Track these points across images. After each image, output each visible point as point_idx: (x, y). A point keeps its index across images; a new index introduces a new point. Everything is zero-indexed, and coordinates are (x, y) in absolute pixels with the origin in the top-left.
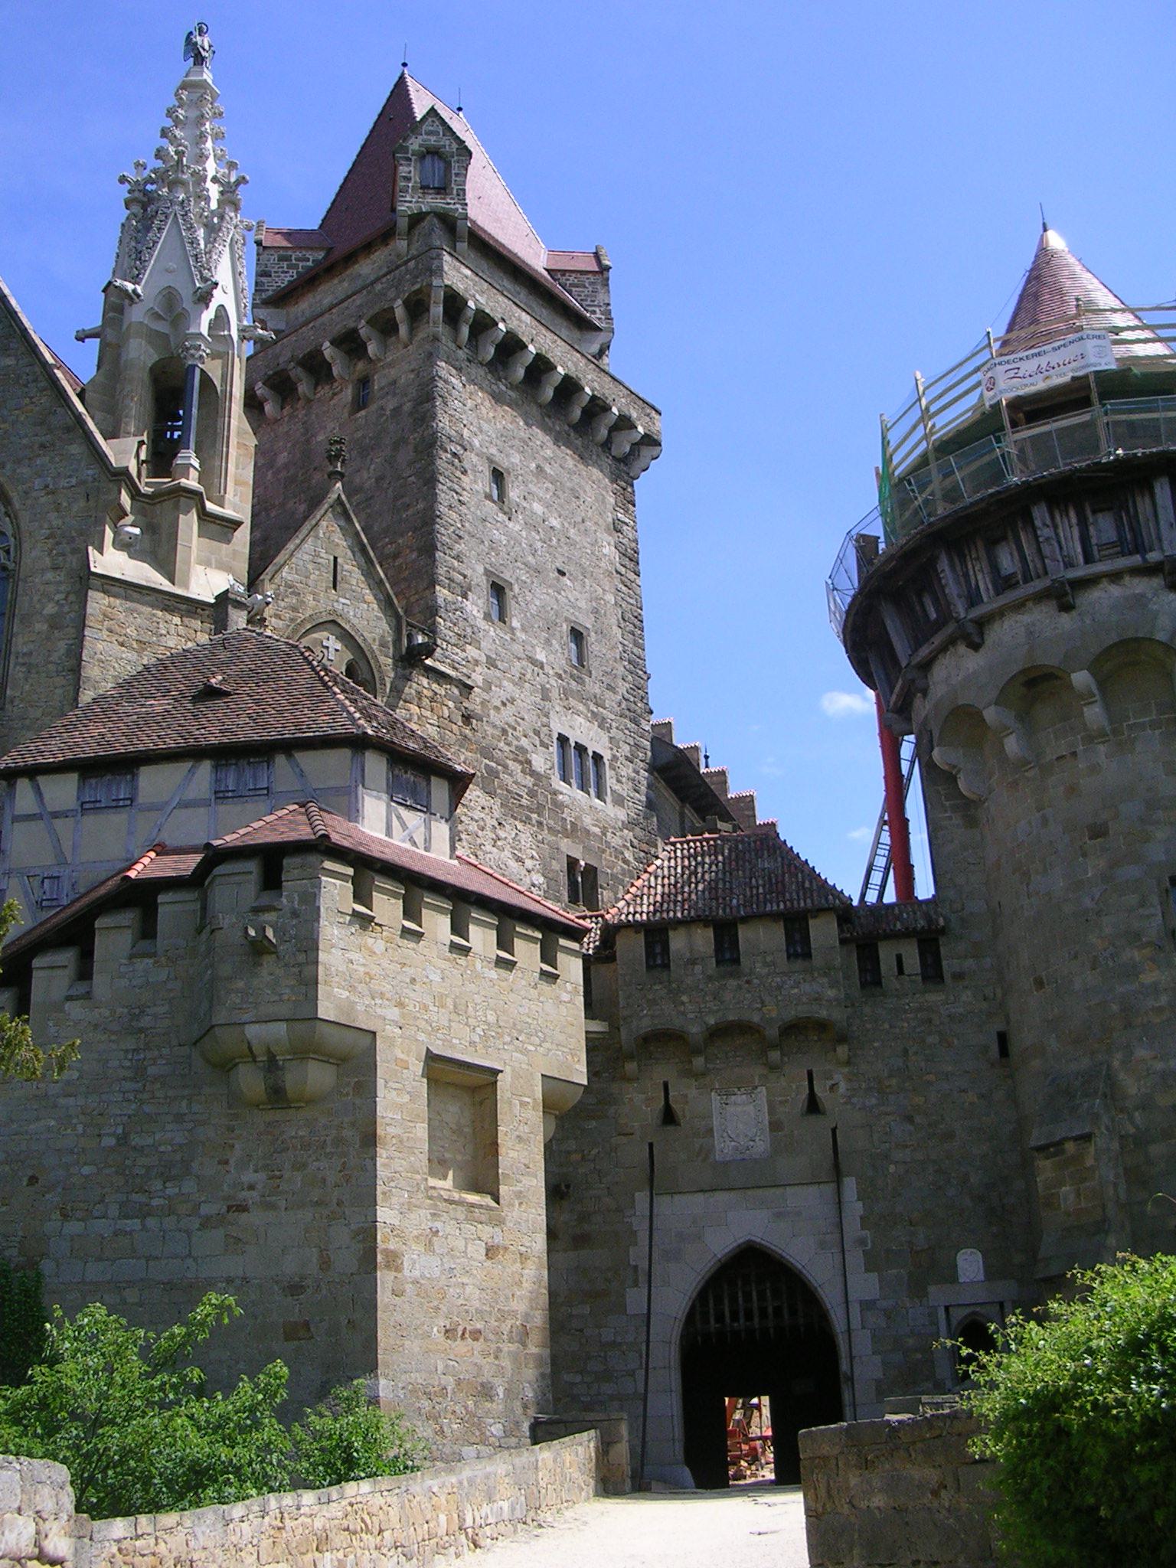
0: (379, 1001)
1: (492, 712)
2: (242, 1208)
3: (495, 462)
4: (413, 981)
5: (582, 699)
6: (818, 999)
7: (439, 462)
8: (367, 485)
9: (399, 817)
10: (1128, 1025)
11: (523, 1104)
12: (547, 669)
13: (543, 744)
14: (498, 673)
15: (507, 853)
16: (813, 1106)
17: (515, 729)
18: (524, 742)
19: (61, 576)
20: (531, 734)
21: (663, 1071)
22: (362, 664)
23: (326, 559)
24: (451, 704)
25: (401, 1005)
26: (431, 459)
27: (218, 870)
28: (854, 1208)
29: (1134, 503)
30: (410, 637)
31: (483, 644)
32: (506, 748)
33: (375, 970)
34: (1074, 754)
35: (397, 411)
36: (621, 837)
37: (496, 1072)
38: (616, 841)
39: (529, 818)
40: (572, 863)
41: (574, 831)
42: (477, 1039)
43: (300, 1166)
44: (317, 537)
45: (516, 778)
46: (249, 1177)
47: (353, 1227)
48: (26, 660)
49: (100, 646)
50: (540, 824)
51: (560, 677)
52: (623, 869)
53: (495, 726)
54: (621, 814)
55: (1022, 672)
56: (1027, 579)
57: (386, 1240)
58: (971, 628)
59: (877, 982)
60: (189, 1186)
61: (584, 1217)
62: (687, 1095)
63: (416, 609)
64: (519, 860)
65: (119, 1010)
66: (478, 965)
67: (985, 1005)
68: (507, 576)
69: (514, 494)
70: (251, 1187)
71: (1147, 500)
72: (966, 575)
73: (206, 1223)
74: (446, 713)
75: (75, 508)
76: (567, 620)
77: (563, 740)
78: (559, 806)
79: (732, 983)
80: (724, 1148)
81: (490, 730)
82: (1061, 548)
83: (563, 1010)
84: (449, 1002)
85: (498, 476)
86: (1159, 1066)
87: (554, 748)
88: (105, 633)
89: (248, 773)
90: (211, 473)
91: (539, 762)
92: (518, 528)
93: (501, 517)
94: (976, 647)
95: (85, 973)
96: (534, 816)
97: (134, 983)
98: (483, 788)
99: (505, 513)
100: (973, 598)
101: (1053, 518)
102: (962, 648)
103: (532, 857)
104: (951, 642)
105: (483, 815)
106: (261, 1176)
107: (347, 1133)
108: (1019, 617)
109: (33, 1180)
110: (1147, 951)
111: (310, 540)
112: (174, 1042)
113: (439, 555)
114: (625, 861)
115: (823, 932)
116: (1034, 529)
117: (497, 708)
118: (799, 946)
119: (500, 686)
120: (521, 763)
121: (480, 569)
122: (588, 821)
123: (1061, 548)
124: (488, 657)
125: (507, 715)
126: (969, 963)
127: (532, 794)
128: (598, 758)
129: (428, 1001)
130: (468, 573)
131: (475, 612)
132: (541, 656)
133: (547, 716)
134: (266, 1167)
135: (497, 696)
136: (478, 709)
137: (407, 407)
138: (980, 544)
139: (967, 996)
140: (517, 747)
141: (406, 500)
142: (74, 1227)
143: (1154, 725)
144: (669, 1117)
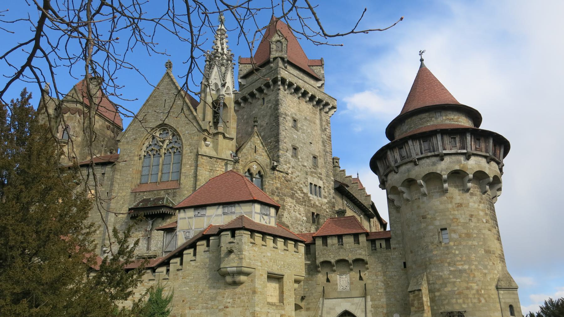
0: (256, 262)
1: (293, 179)
2: (227, 307)
3: (295, 118)
4: (264, 256)
5: (315, 173)
6: (360, 254)
7: (280, 120)
8: (264, 125)
9: (263, 217)
10: (431, 264)
11: (289, 282)
12: (307, 167)
13: (306, 186)
14: (295, 170)
15: (297, 213)
16: (361, 278)
17: (299, 183)
18: (301, 186)
19: (192, 154)
20: (303, 183)
21: (326, 270)
22: (262, 171)
23: (253, 147)
24: (283, 178)
25: (261, 262)
26: (278, 120)
27: (222, 233)
28: (369, 303)
29: (433, 139)
30: (273, 163)
31: (291, 163)
32: (297, 188)
33: (256, 255)
34: (419, 198)
35: (271, 107)
36: (326, 206)
37: (283, 276)
38: (324, 207)
39: (302, 204)
40: (313, 213)
41: (314, 206)
42: (279, 268)
43: (239, 298)
44: (251, 141)
45: (299, 195)
46: (229, 300)
47: (250, 312)
48: (185, 174)
49: (201, 172)
50: (305, 205)
51: (310, 169)
52: (326, 214)
53: (294, 183)
54: (326, 201)
55: (407, 179)
56: (408, 158)
57: (257, 314)
58: (395, 169)
59: (376, 250)
60: (216, 302)
61: (308, 304)
62: (332, 276)
63: (275, 156)
64: (300, 214)
65: (202, 263)
66: (279, 251)
67: (401, 256)
68: (297, 145)
69: (299, 125)
70: (229, 303)
71: (436, 139)
72: (394, 156)
73: (220, 310)
75: (195, 138)
76: (312, 155)
77: (311, 184)
78: (310, 200)
79: (342, 250)
80: (340, 288)
81: (293, 184)
82: (415, 151)
83: (300, 260)
84: (273, 261)
85: (295, 121)
86: (437, 274)
87: (309, 187)
88: (202, 168)
89: (230, 208)
90: (226, 127)
91: (306, 190)
92: (300, 133)
93: (296, 131)
94: (397, 173)
95: (195, 255)
96: (304, 203)
97: (205, 257)
98: (291, 198)
99: (297, 130)
100: (396, 161)
101: (413, 143)
102: (393, 172)
103: (303, 213)
104: (390, 172)
105: (291, 204)
106: (231, 300)
107: (249, 291)
108: (406, 166)
109: (183, 301)
110: (435, 246)
111: (249, 142)
112: (213, 270)
113: (280, 143)
114: (327, 212)
115: (362, 239)
116: (409, 146)
117: (295, 178)
118: (357, 241)
119: (295, 173)
120: (300, 191)
121: (291, 145)
122: (317, 203)
123: (415, 151)
124: (292, 166)
125: (297, 179)
126: (397, 246)
127: (303, 198)
128: (320, 187)
129: (268, 260)
130: (288, 146)
132: (305, 164)
133: (307, 179)
134: (232, 298)
135: (294, 176)
136: (290, 179)
137: (273, 106)
138: (397, 148)
139: (396, 253)
141: (273, 129)
142: (192, 311)
143: (437, 192)
144: (328, 280)
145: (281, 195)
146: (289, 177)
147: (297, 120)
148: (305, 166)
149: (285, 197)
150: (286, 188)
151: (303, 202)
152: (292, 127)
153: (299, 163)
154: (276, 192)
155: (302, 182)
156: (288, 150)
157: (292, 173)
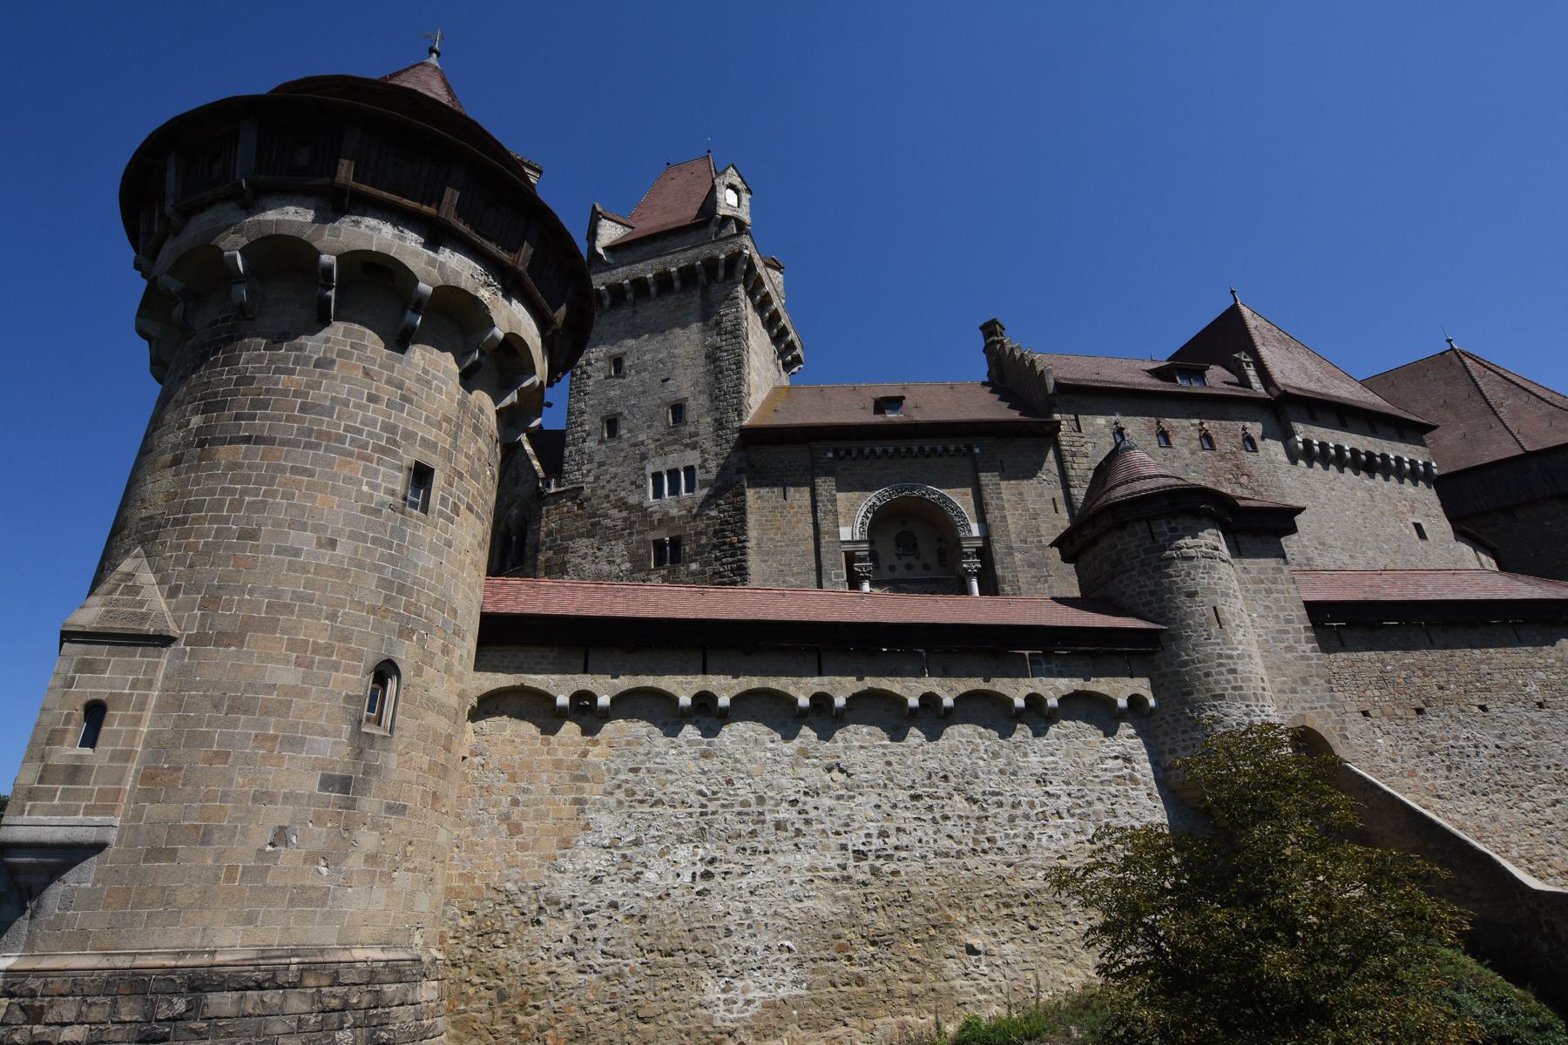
5: (675, 442)
13: (637, 487)
18: (623, 494)
24: (569, 503)
51: (659, 440)
53: (600, 497)
68: (619, 410)
74: (565, 509)
76: (667, 404)
91: (633, 500)
122: (674, 512)
125: (612, 486)
131: (592, 445)
132: (642, 437)
133: (643, 469)
140: (616, 501)
145: (559, 542)
146: (587, 491)
147: (625, 353)
148: (642, 443)
149: (570, 543)
150: (575, 521)
151: (622, 530)
152: (609, 377)
153: (625, 445)
154: (545, 543)
155: (627, 484)
156: (588, 435)
157: (597, 478)
